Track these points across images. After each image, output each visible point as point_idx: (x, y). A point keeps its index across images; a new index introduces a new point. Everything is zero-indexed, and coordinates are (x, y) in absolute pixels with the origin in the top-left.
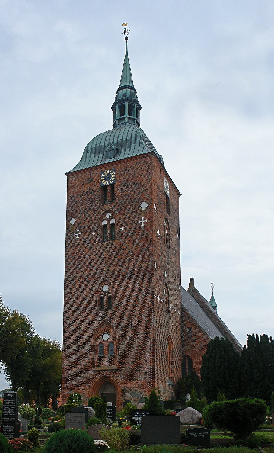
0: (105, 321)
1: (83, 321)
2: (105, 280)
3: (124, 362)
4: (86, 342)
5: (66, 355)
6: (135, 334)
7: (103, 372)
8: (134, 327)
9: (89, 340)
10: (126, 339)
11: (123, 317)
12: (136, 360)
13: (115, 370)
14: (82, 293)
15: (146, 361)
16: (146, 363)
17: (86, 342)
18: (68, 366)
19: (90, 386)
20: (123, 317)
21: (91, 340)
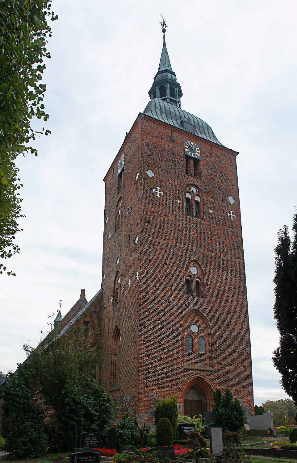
0: (196, 310)
1: (169, 302)
2: (194, 261)
3: (221, 364)
4: (173, 330)
5: (144, 341)
6: (231, 333)
7: (197, 372)
8: (230, 325)
9: (177, 328)
10: (222, 337)
11: (217, 310)
12: (233, 363)
13: (211, 371)
14: (166, 266)
15: (244, 366)
16: (244, 368)
17: (173, 330)
18: (149, 357)
19: (179, 388)
20: (217, 310)
21: (180, 329)
